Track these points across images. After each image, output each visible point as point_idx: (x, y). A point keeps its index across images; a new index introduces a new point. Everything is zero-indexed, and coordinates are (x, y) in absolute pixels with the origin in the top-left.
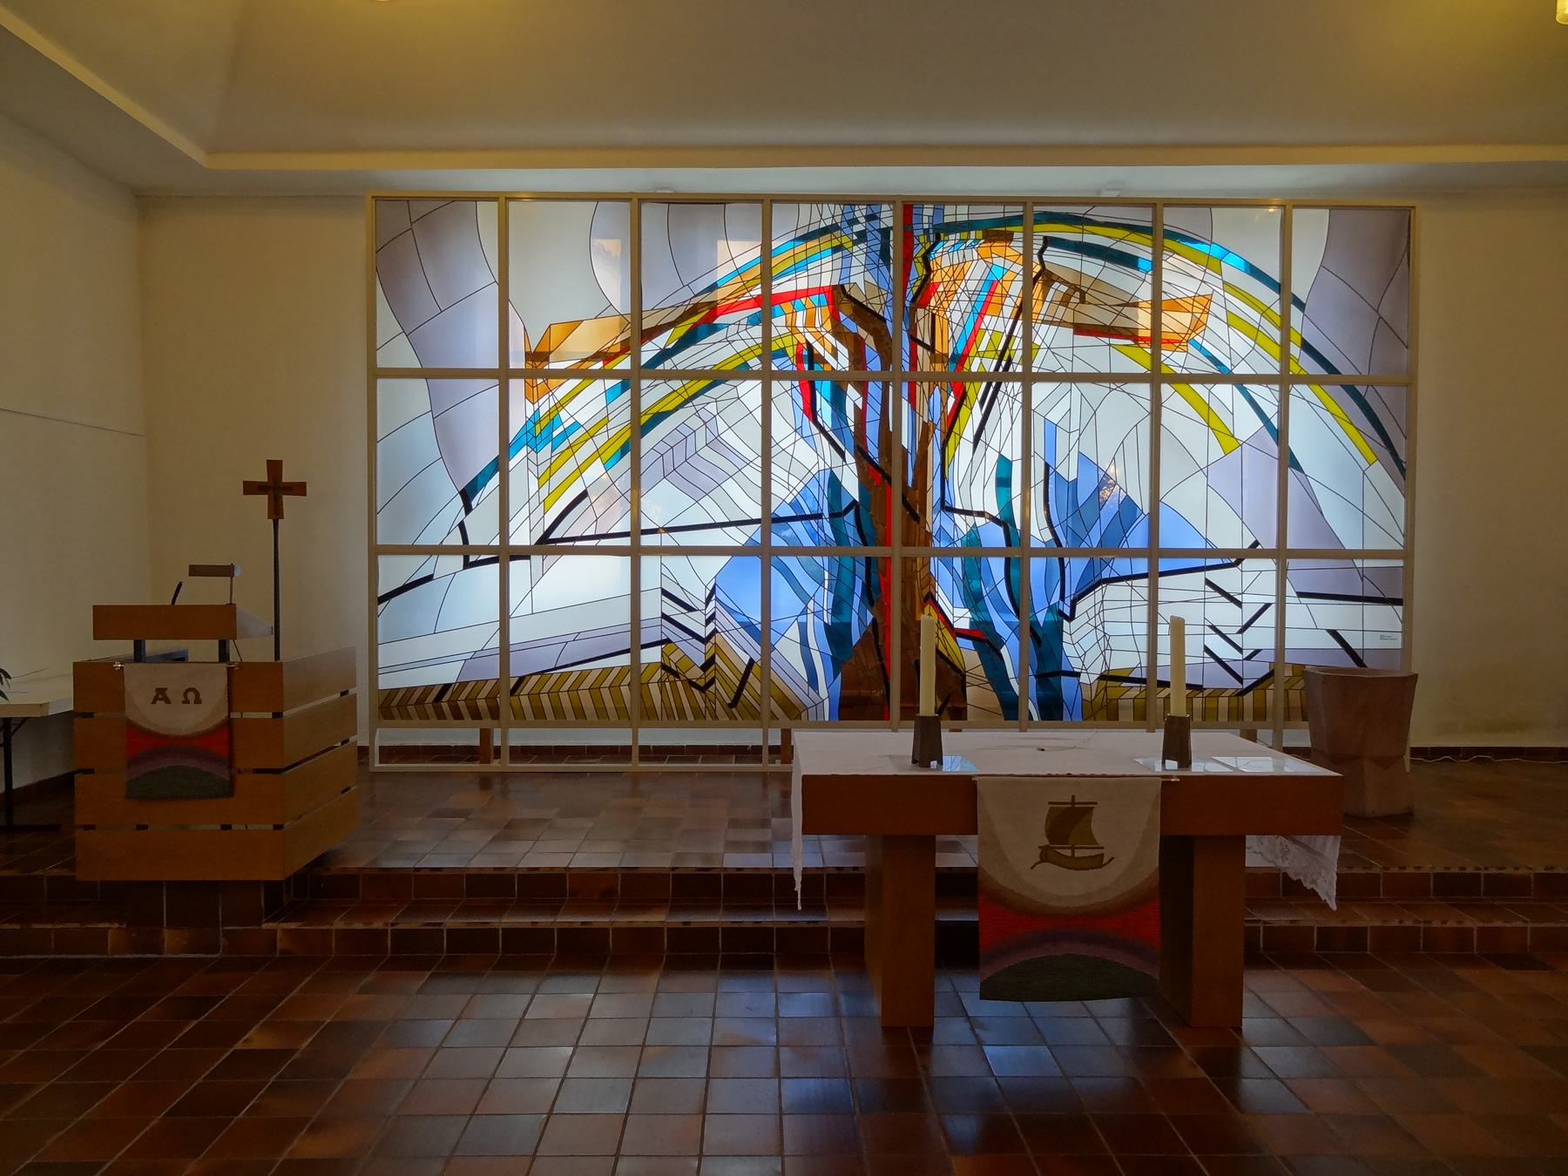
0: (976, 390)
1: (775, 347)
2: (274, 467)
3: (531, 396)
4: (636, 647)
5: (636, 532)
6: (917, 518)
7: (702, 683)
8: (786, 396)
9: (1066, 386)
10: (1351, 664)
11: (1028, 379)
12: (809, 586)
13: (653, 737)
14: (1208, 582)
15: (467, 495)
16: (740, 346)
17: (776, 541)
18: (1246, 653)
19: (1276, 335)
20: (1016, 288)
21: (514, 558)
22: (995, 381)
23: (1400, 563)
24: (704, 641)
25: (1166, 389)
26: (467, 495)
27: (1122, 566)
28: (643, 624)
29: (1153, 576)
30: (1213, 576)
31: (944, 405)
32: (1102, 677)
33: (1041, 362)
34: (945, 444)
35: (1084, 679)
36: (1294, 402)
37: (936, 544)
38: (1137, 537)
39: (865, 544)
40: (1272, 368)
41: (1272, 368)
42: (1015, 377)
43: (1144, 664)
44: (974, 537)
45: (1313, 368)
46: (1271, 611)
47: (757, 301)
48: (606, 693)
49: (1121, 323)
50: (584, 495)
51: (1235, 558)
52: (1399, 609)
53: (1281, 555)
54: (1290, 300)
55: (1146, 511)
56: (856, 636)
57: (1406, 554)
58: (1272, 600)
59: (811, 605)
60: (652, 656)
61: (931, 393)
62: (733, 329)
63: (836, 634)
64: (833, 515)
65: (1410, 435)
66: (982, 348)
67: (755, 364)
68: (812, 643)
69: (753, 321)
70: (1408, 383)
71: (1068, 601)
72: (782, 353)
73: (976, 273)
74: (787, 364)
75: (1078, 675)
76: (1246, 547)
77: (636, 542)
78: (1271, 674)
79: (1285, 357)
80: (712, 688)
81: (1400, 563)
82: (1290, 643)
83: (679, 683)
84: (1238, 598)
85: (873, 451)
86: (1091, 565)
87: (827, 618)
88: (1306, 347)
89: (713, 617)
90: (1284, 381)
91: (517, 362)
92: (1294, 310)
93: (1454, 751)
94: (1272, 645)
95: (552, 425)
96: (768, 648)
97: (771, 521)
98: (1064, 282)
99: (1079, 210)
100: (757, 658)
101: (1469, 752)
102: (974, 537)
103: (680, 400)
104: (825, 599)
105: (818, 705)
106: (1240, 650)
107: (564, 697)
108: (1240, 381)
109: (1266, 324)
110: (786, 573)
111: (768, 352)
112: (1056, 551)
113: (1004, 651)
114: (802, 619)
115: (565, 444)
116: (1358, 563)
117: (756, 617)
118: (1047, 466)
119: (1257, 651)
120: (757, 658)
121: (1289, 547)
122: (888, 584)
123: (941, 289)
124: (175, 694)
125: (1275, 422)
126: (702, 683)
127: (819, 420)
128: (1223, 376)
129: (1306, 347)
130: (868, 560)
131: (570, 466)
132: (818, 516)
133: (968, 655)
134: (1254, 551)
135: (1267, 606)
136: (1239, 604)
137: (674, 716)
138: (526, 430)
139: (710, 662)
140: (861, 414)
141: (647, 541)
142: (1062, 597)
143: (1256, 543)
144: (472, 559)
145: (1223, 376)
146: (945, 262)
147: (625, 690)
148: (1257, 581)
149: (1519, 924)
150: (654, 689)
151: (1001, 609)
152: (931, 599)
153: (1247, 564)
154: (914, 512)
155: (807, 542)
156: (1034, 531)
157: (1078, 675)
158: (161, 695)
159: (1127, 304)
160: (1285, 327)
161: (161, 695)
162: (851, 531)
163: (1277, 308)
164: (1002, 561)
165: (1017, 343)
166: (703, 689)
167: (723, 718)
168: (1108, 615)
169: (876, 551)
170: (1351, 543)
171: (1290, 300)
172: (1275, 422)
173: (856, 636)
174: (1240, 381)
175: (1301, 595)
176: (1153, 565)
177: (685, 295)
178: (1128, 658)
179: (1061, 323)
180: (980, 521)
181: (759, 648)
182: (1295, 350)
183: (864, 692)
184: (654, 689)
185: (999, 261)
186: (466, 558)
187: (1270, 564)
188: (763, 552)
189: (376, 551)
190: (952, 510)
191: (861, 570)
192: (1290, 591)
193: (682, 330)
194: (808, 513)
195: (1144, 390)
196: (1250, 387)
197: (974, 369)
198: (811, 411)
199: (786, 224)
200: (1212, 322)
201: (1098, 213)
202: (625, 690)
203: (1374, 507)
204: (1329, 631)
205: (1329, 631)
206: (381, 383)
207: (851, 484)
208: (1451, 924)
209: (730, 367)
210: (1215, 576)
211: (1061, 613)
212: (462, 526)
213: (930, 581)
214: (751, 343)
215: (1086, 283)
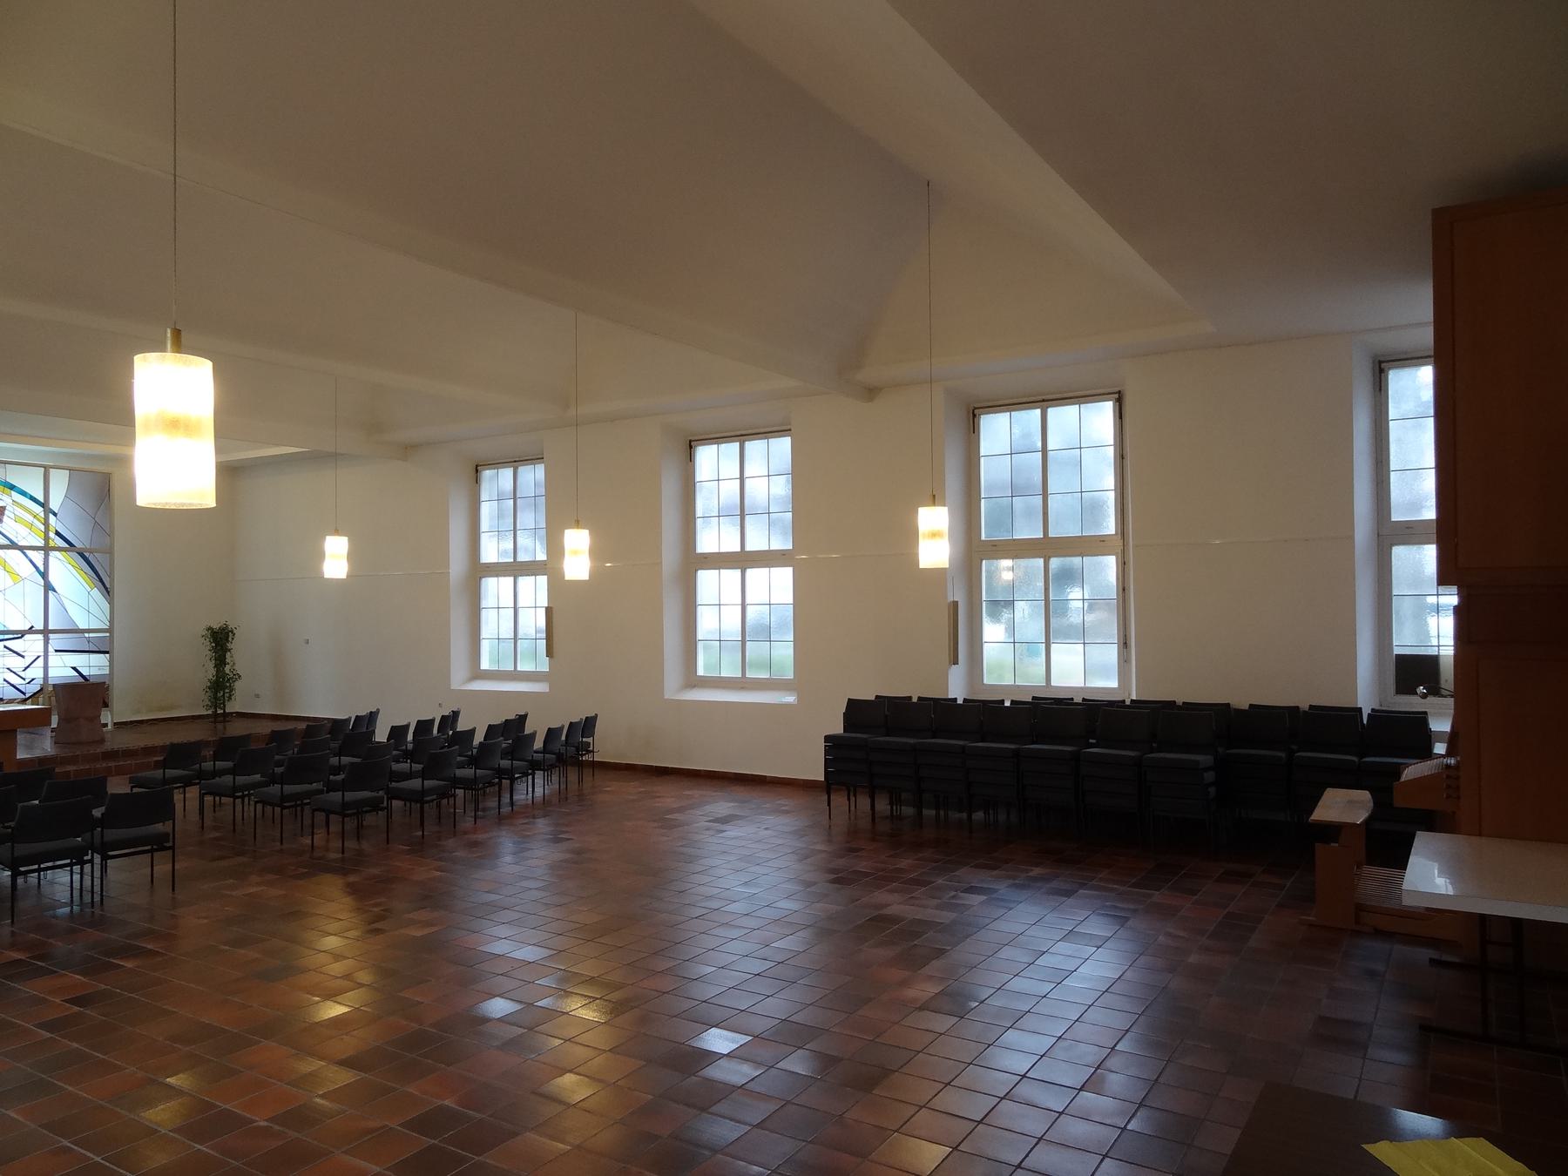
10: (82, 680)
14: (5, 647)
18: (27, 681)
19: (42, 528)
23: (108, 634)
30: (7, 643)
36: (50, 558)
40: (41, 543)
41: (41, 543)
45: (61, 543)
46: (41, 659)
51: (21, 634)
52: (107, 655)
53: (46, 632)
54: (48, 510)
57: (110, 630)
58: (42, 654)
65: (111, 576)
70: (110, 551)
76: (27, 628)
78: (42, 689)
79: (47, 538)
81: (108, 634)
82: (51, 673)
84: (23, 654)
88: (57, 533)
90: (46, 549)
93: (141, 722)
106: (24, 679)
108: (22, 549)
109: (36, 521)
116: (87, 635)
119: (33, 679)
121: (50, 628)
125: (42, 569)
129: (57, 533)
134: (31, 630)
135: (38, 657)
136: (23, 657)
143: (32, 627)
145: (13, 545)
148: (33, 644)
149: (129, 762)
160: (46, 524)
163: (42, 515)
170: (82, 624)
171: (48, 510)
172: (42, 569)
174: (22, 549)
175: (56, 651)
182: (52, 535)
187: (40, 637)
192: (51, 649)
196: (26, 551)
203: (94, 609)
204: (72, 668)
205: (72, 668)
208: (104, 765)
210: (8, 644)
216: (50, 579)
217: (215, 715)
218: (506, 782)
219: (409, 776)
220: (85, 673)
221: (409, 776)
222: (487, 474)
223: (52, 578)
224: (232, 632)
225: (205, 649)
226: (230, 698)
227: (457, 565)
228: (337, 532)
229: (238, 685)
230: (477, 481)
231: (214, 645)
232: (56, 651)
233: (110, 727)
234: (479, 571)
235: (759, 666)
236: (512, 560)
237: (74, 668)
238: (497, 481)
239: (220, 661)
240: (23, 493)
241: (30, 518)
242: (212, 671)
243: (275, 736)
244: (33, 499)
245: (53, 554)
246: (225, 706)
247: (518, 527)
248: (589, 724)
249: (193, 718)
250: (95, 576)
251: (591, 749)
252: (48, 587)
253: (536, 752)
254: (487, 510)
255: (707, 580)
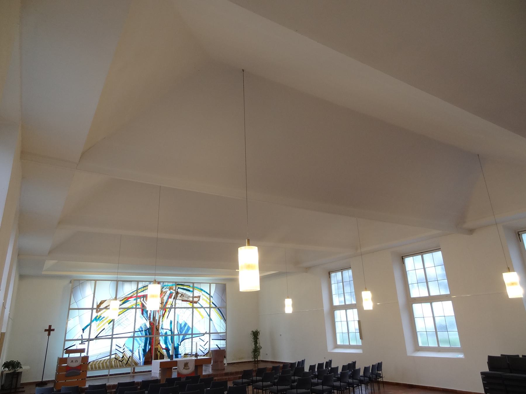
0: (167, 310)
1: (138, 304)
2: (50, 326)
3: (97, 312)
4: (111, 355)
5: (113, 335)
6: (158, 330)
7: (121, 361)
8: (139, 311)
9: (180, 309)
11: (175, 308)
12: (140, 342)
13: (113, 371)
15: (83, 330)
16: (132, 304)
17: (136, 335)
18: (205, 349)
19: (209, 301)
20: (174, 295)
21: (90, 340)
22: (170, 308)
23: (225, 334)
24: (123, 353)
25: (194, 309)
26: (83, 330)
27: (188, 336)
28: (112, 351)
29: (192, 338)
30: (200, 337)
31: (163, 312)
32: (184, 354)
33: (177, 306)
34: (163, 318)
35: (182, 355)
37: (161, 334)
38: (190, 332)
39: (150, 335)
40: (208, 306)
41: (208, 306)
42: (173, 308)
43: (191, 352)
44: (166, 333)
45: (213, 306)
46: (208, 342)
47: (135, 297)
48: (104, 364)
49: (188, 300)
50: (104, 329)
52: (225, 341)
53: (210, 333)
54: (211, 296)
55: (191, 327)
56: (147, 350)
57: (226, 333)
58: (209, 340)
59: (140, 346)
60: (113, 356)
61: (161, 311)
62: (131, 301)
63: (144, 350)
64: (145, 330)
65: (226, 315)
66: (169, 304)
67: (134, 306)
68: (140, 352)
69: (134, 300)
71: (180, 342)
72: (139, 304)
73: (169, 292)
74: (139, 307)
75: (181, 354)
76: (205, 332)
77: (112, 336)
78: (208, 352)
79: (210, 304)
80: (123, 361)
81: (225, 334)
83: (117, 361)
85: (152, 320)
86: (183, 337)
87: (143, 348)
88: (213, 303)
89: (124, 349)
90: (210, 308)
91: (95, 306)
92: (211, 298)
94: (208, 348)
95: (100, 317)
96: (133, 353)
97: (135, 332)
98: (181, 294)
99: (183, 283)
100: (131, 355)
101: (236, 363)
102: (166, 333)
103: (122, 312)
104: (143, 344)
105: (140, 363)
107: (97, 365)
108: (204, 308)
110: (136, 340)
111: (136, 305)
112: (179, 335)
113: (170, 351)
114: (139, 348)
115: (102, 320)
116: (220, 334)
117: (131, 349)
118: (177, 321)
120: (131, 355)
122: (153, 342)
123: (163, 295)
124: (74, 361)
125: (209, 314)
126: (121, 361)
127: (144, 315)
128: (202, 307)
129: (213, 303)
130: (150, 338)
131: (102, 324)
132: (143, 331)
133: (164, 352)
135: (208, 341)
137: (116, 367)
138: (96, 318)
139: (123, 357)
140: (150, 314)
141: (114, 336)
142: (179, 342)
144: (83, 341)
145: (202, 307)
146: (164, 291)
147: (108, 363)
148: (206, 338)
150: (113, 362)
151: (170, 345)
152: (159, 343)
153: (205, 335)
154: (158, 330)
155: (141, 335)
156: (175, 332)
157: (181, 354)
158: (72, 361)
159: (189, 297)
160: (210, 300)
161: (72, 361)
162: (148, 333)
163: (209, 297)
164: (170, 336)
165: (174, 303)
166: (121, 362)
167: (125, 366)
168: (185, 344)
169: (151, 336)
170: (219, 331)
171: (211, 296)
172: (209, 314)
173: (147, 350)
174: (204, 308)
175: (212, 339)
176: (192, 336)
177: (124, 295)
178: (188, 351)
179: (180, 300)
180: (167, 331)
181: (131, 354)
182: (211, 303)
183: (148, 360)
184: (113, 362)
185: (171, 291)
186: (82, 341)
187: (208, 335)
188: (134, 337)
189: (66, 340)
190: (163, 329)
191: (149, 339)
192: (211, 339)
193: (123, 301)
194: (141, 330)
195: (191, 309)
196: (205, 309)
197: (167, 307)
198: (143, 314)
199: (141, 285)
200: (200, 299)
201: (185, 284)
202: (108, 363)
203: (222, 326)
206: (70, 311)
207: (148, 326)
208: (225, 378)
209: (130, 307)
210: (201, 337)
211: (179, 345)
212: (82, 335)
213: (159, 341)
214: (134, 303)
215: (184, 294)
216: (211, 317)
217: (255, 361)
218: (351, 388)
219: (317, 384)
220: (219, 347)
221: (317, 384)
222: (333, 275)
223: (211, 317)
224: (259, 332)
225: (251, 338)
226: (259, 354)
227: (326, 307)
228: (288, 297)
229: (261, 351)
230: (330, 277)
231: (254, 337)
232: (212, 339)
233: (226, 365)
234: (333, 308)
235: (445, 342)
236: (344, 304)
237: (217, 345)
238: (336, 277)
239: (256, 342)
240: (205, 291)
241: (206, 299)
242: (254, 346)
243: (274, 368)
244: (207, 293)
245: (212, 309)
246: (257, 358)
247: (345, 292)
248: (379, 366)
249: (249, 362)
250: (222, 315)
251: (381, 376)
252: (210, 320)
253: (361, 376)
254: (334, 287)
255: (417, 307)
